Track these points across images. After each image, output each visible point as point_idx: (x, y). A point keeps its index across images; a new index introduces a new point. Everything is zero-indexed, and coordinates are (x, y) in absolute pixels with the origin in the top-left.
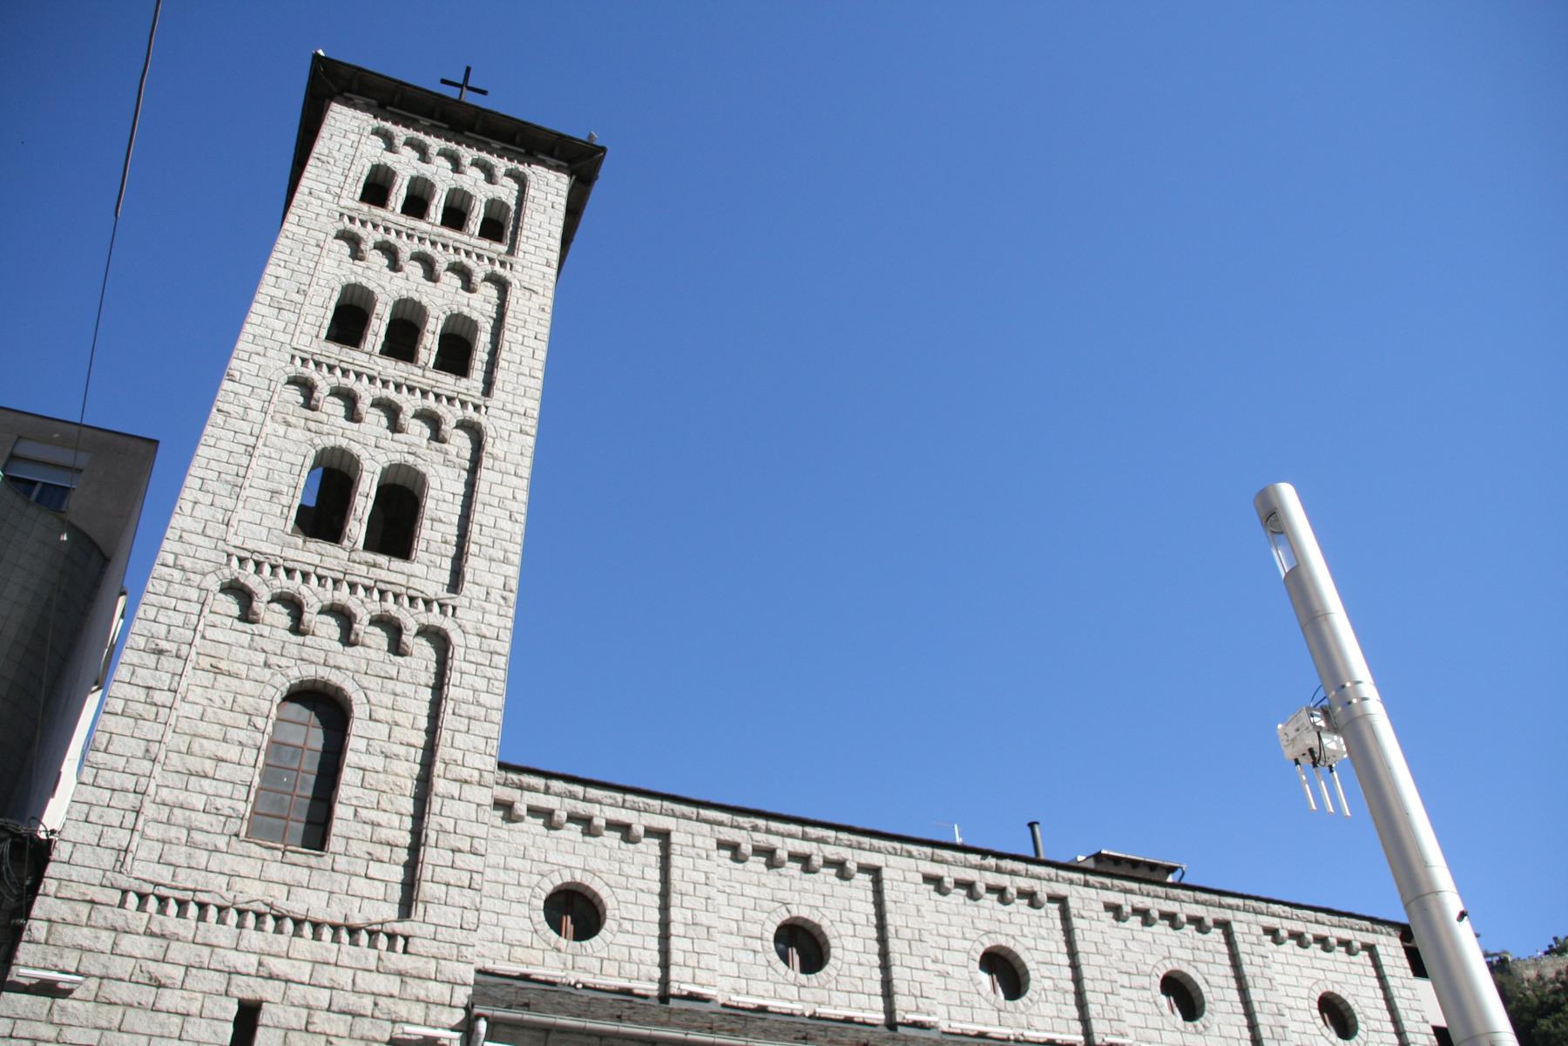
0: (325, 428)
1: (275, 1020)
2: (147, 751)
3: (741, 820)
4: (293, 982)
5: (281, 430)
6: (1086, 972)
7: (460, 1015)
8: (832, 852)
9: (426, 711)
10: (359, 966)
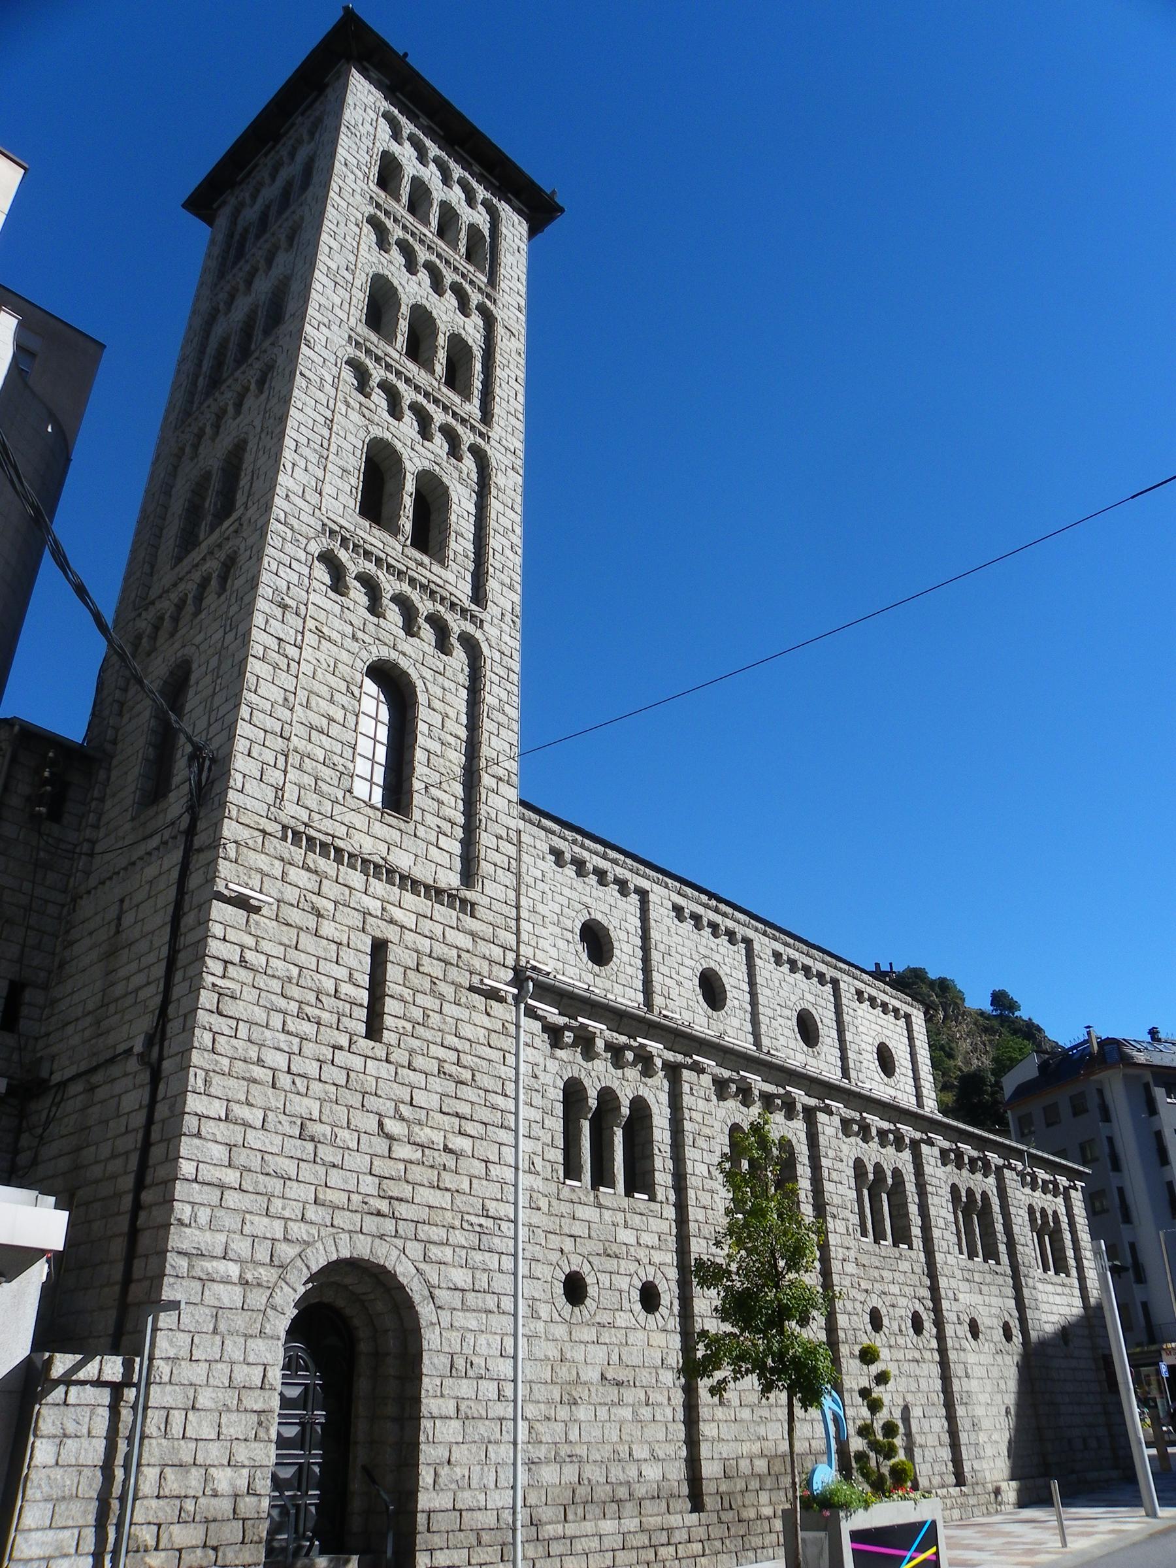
0: (376, 419)
2: (286, 699)
3: (568, 834)
4: (406, 928)
5: (343, 408)
6: (762, 1000)
7: (510, 975)
8: (621, 872)
9: (464, 710)
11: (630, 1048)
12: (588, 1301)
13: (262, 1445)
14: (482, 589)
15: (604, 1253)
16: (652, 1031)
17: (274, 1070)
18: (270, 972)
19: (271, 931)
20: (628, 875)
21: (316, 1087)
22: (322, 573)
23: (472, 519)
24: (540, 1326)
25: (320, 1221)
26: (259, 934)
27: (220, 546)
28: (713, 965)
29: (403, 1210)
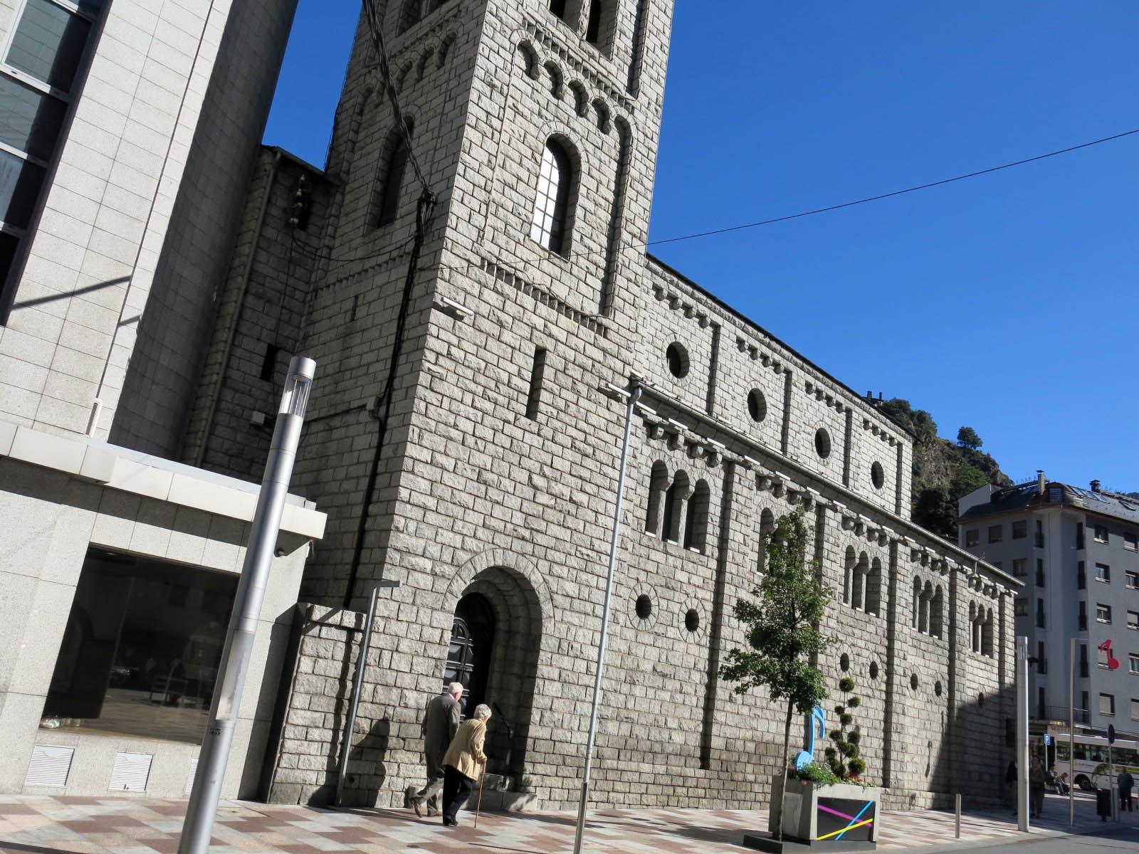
2: (489, 161)
6: (792, 417)
7: (626, 383)
8: (703, 309)
9: (614, 179)
11: (701, 444)
12: (651, 617)
13: (437, 680)
14: (635, 81)
16: (719, 434)
17: (464, 433)
18: (466, 363)
19: (469, 334)
20: (707, 311)
21: (490, 447)
22: (520, 60)
23: (634, 19)
24: (618, 628)
25: (485, 539)
26: (461, 335)
27: (441, 26)
28: (760, 387)
29: (539, 538)
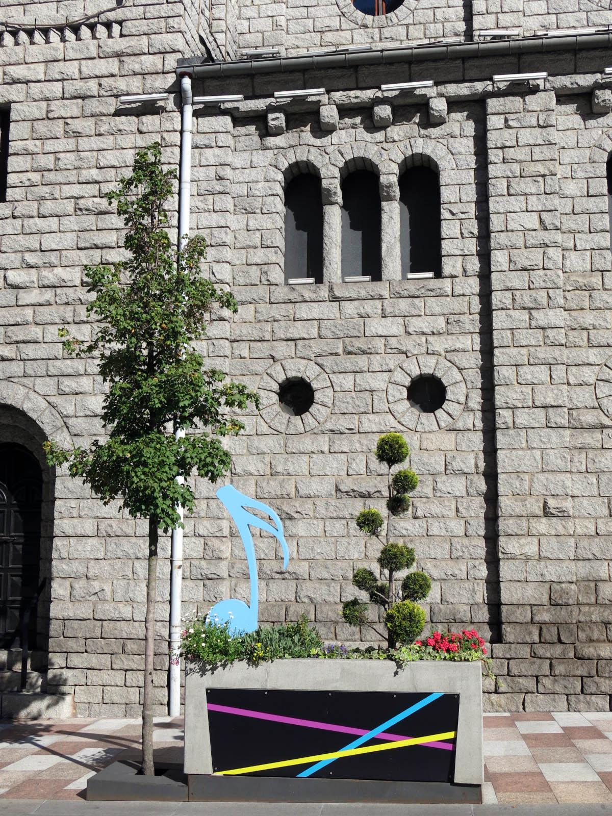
1: (22, 116)
10: (82, 57)
15: (344, 351)
16: (415, 68)
